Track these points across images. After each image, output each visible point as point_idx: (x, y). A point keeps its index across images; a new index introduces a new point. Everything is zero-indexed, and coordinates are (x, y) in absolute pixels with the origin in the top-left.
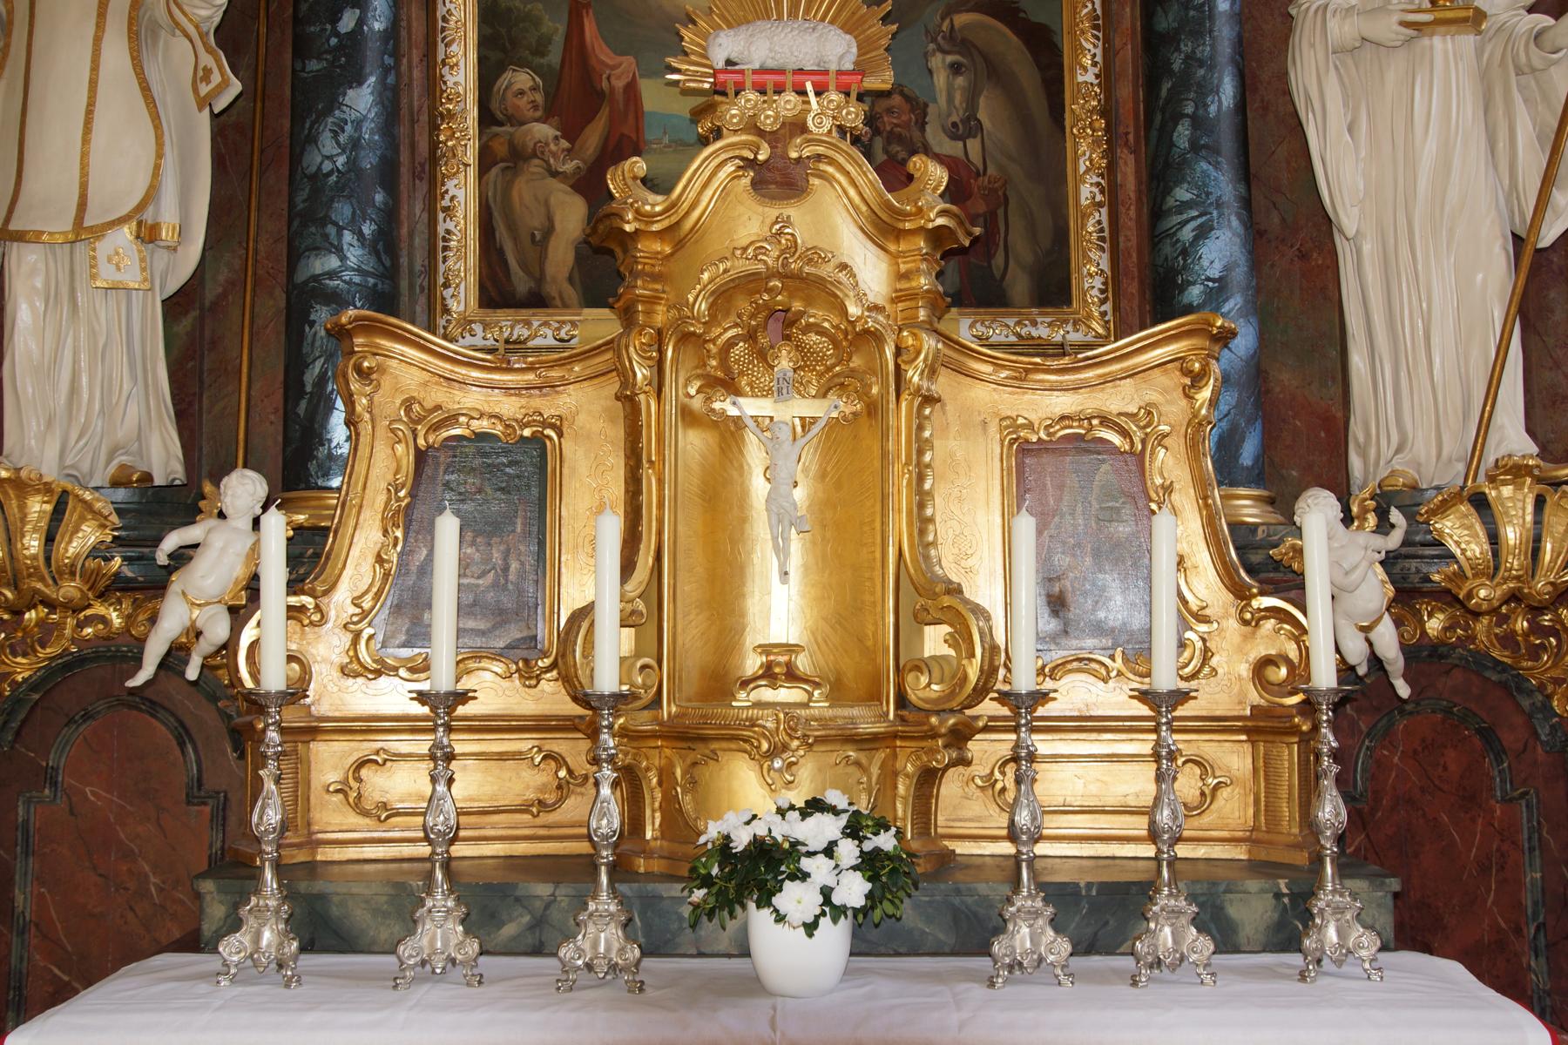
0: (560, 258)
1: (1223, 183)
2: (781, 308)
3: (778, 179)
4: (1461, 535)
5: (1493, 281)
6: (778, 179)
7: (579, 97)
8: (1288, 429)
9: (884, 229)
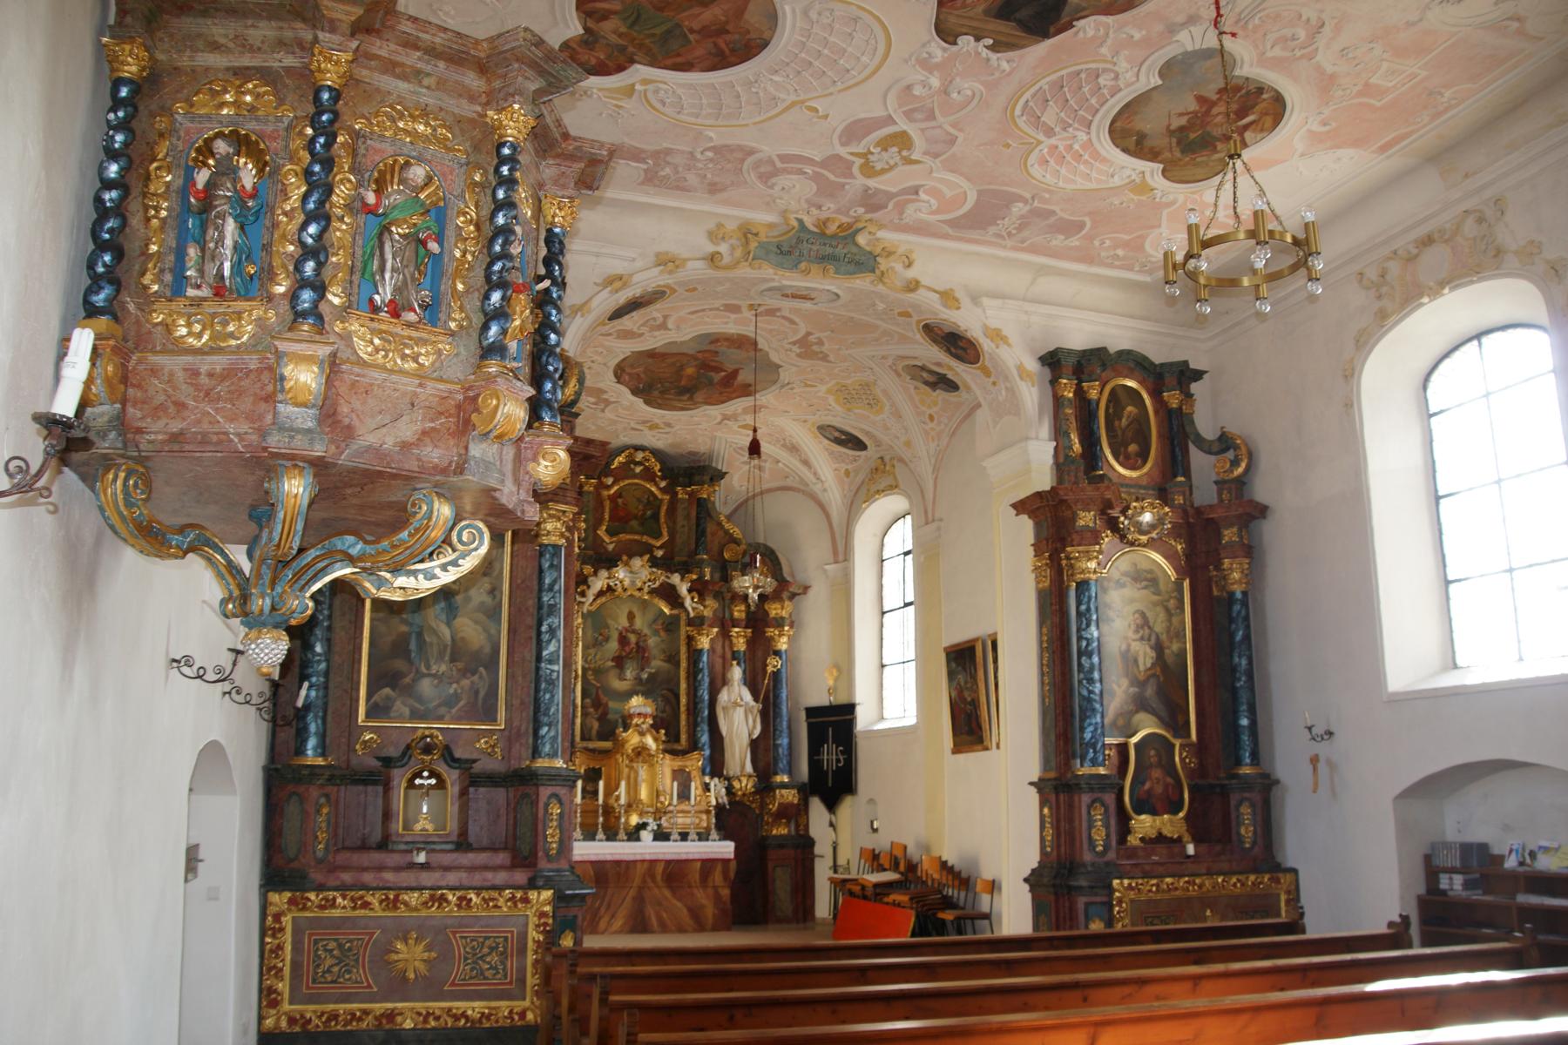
0: (594, 732)
1: (706, 728)
2: (641, 751)
3: (642, 734)
4: (736, 784)
5: (746, 741)
6: (642, 734)
7: (597, 704)
8: (716, 766)
9: (656, 740)
